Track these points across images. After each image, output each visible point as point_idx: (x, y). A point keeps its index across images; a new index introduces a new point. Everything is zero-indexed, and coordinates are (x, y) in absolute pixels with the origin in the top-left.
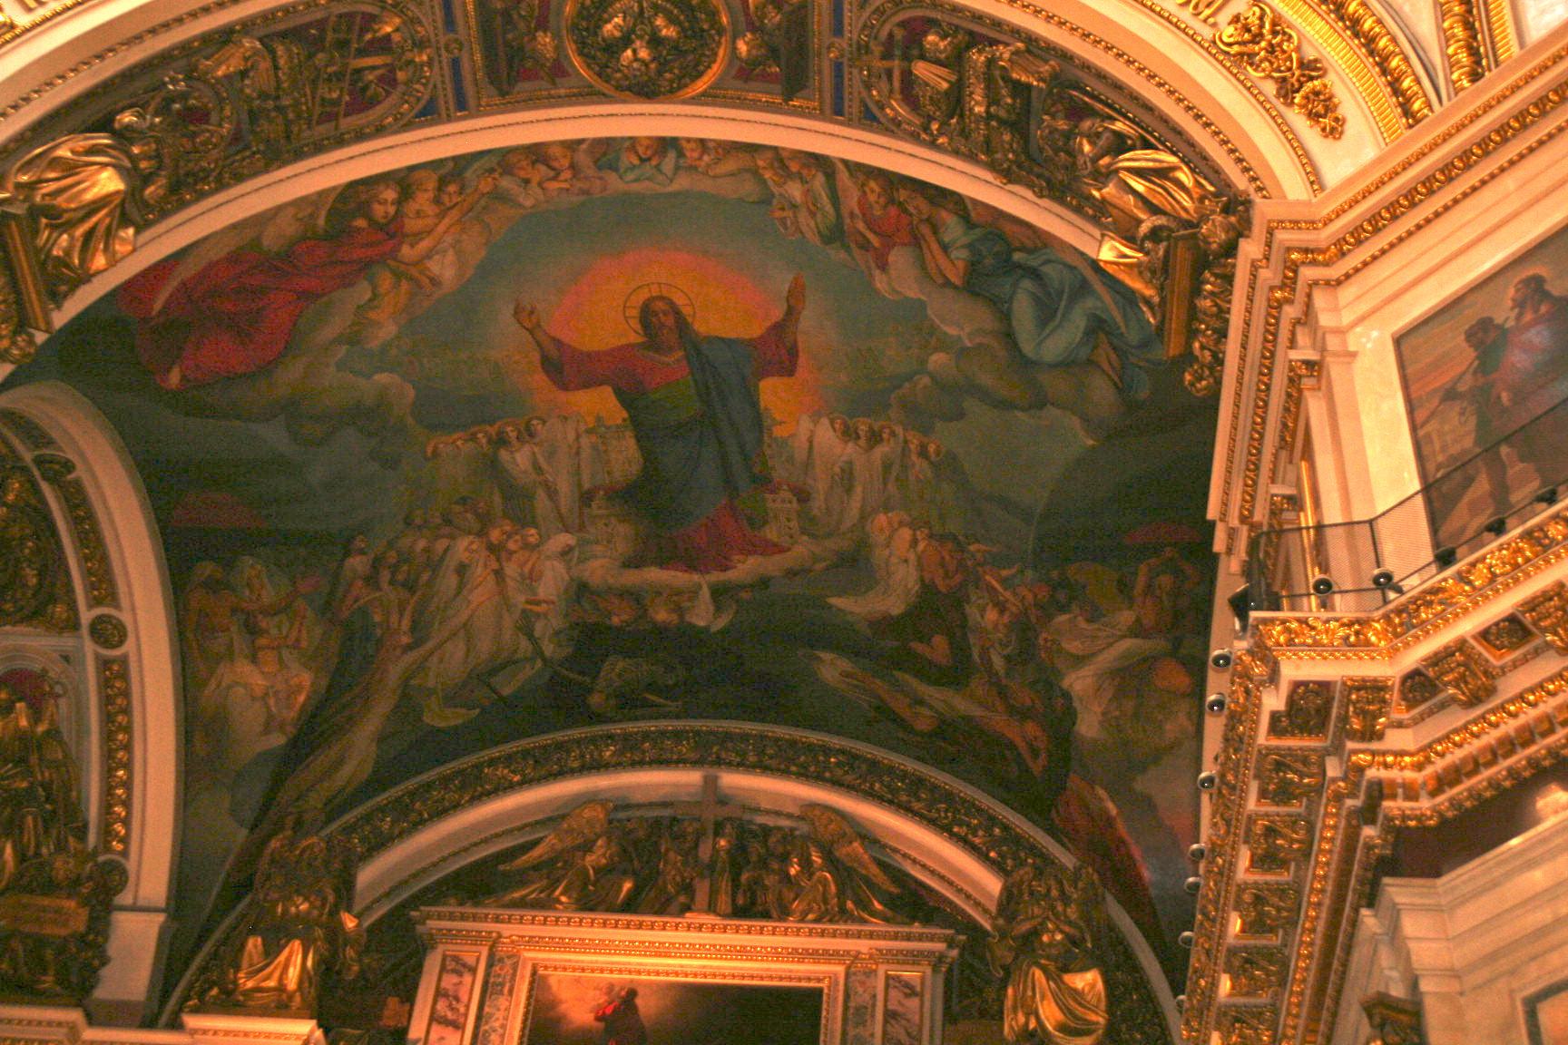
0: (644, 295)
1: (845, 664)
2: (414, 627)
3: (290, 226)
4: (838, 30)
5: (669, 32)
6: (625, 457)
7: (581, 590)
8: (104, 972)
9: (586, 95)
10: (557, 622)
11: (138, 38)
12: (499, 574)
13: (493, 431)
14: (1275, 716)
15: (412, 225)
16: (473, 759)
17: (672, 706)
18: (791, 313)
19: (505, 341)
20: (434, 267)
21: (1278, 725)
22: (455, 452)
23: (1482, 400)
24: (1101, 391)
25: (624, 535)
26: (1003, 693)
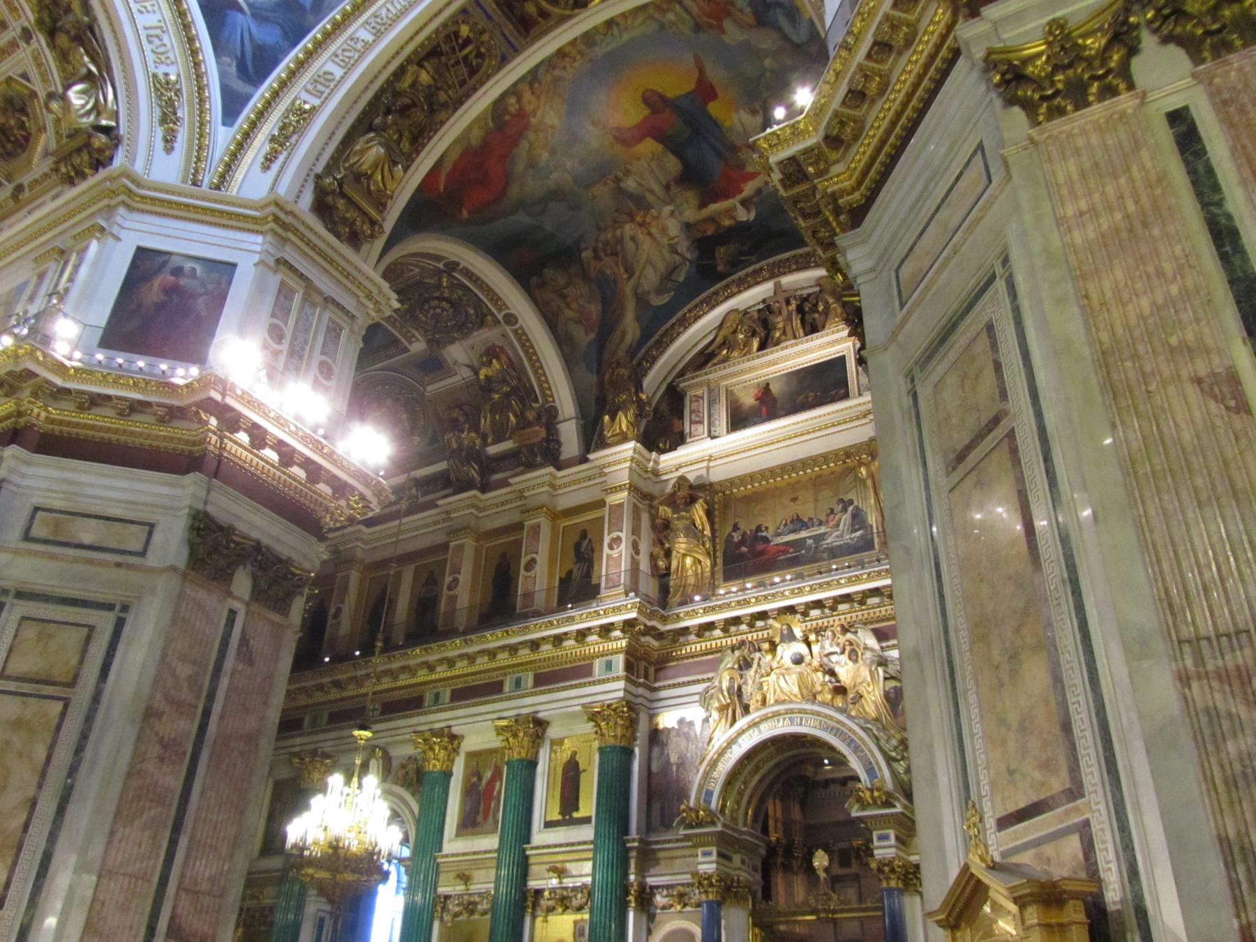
0: (642, 90)
2: (626, 270)
6: (673, 165)
7: (688, 227)
8: (562, 448)
9: (564, 19)
11: (367, 88)
12: (649, 234)
13: (612, 177)
14: (781, 181)
15: (529, 108)
16: (680, 314)
17: (753, 258)
18: (701, 71)
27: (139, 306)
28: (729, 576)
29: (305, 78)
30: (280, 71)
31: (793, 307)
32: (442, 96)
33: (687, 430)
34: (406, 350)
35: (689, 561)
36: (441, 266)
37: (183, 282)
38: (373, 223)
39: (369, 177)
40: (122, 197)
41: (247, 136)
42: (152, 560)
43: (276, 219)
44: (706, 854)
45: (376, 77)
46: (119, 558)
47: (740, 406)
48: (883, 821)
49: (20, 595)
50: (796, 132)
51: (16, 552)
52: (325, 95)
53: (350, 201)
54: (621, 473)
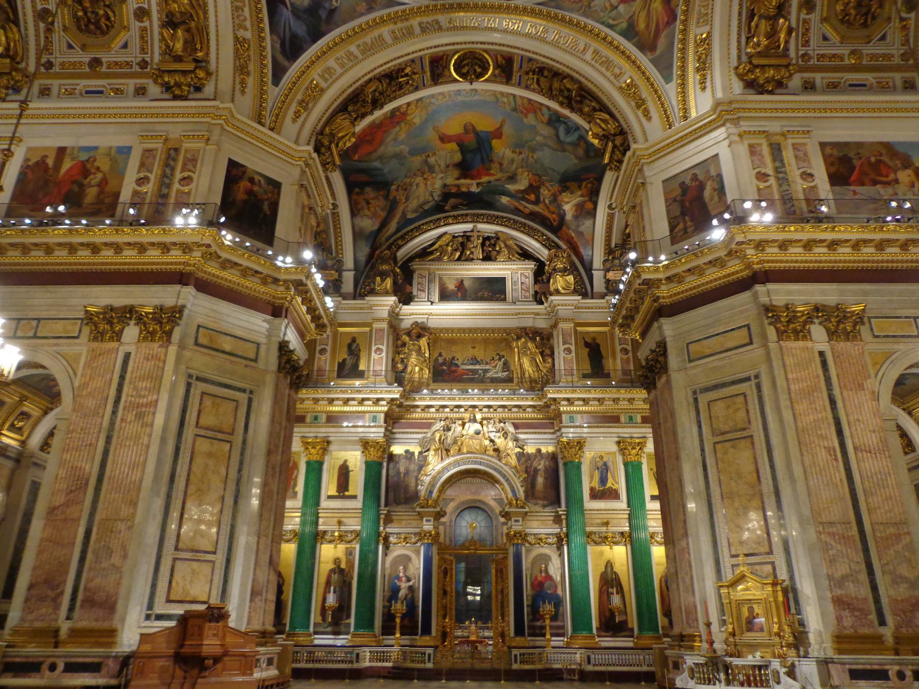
1: (508, 199)
3: (382, 118)
4: (521, 67)
5: (479, 70)
6: (458, 157)
7: (445, 185)
10: (439, 193)
15: (409, 112)
18: (501, 126)
19: (431, 135)
20: (415, 121)
21: (639, 285)
22: (417, 161)
23: (682, 203)
24: (581, 152)
25: (456, 173)
26: (548, 208)
28: (434, 381)
31: (480, 241)
33: (415, 292)
35: (417, 369)
37: (256, 188)
42: (261, 365)
44: (427, 521)
45: (357, 81)
47: (446, 288)
48: (517, 514)
49: (198, 379)
50: (657, 270)
52: (329, 82)
54: (384, 313)
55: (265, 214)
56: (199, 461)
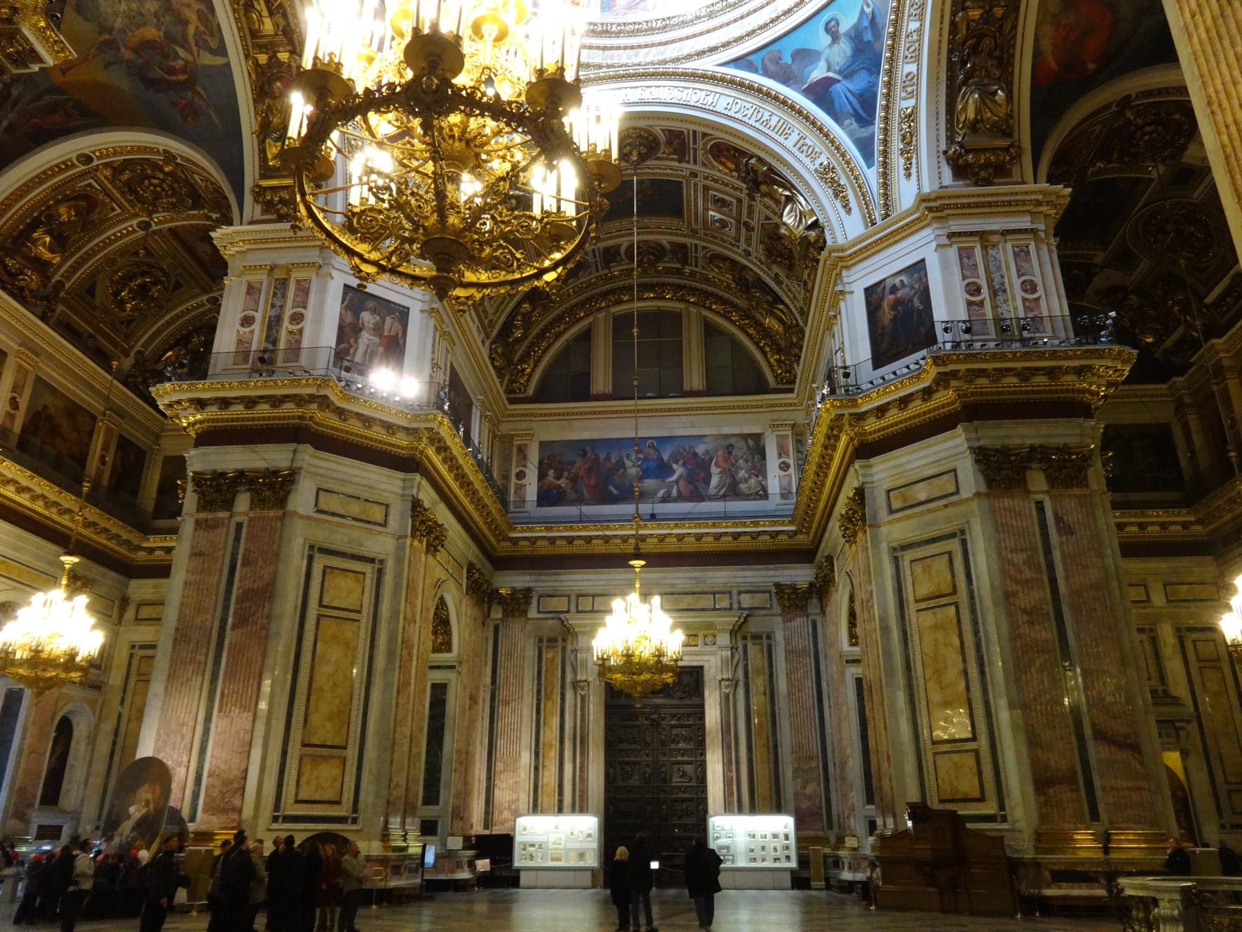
27: (883, 328)
29: (899, 92)
30: (880, 102)
32: (999, 12)
34: (1151, 180)
36: (1114, 109)
37: (899, 294)
38: (1006, 150)
39: (982, 121)
40: (840, 264)
41: (885, 164)
42: (966, 493)
43: (930, 209)
46: (944, 502)
51: (890, 522)
53: (976, 151)
55: (920, 312)
56: (928, 639)
